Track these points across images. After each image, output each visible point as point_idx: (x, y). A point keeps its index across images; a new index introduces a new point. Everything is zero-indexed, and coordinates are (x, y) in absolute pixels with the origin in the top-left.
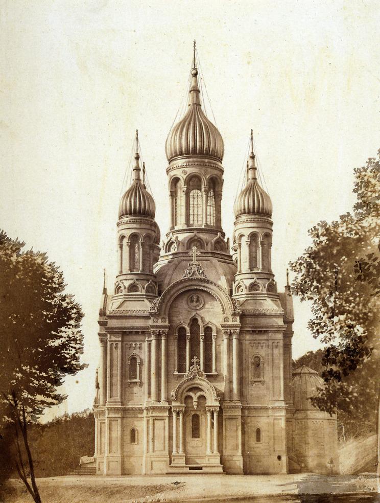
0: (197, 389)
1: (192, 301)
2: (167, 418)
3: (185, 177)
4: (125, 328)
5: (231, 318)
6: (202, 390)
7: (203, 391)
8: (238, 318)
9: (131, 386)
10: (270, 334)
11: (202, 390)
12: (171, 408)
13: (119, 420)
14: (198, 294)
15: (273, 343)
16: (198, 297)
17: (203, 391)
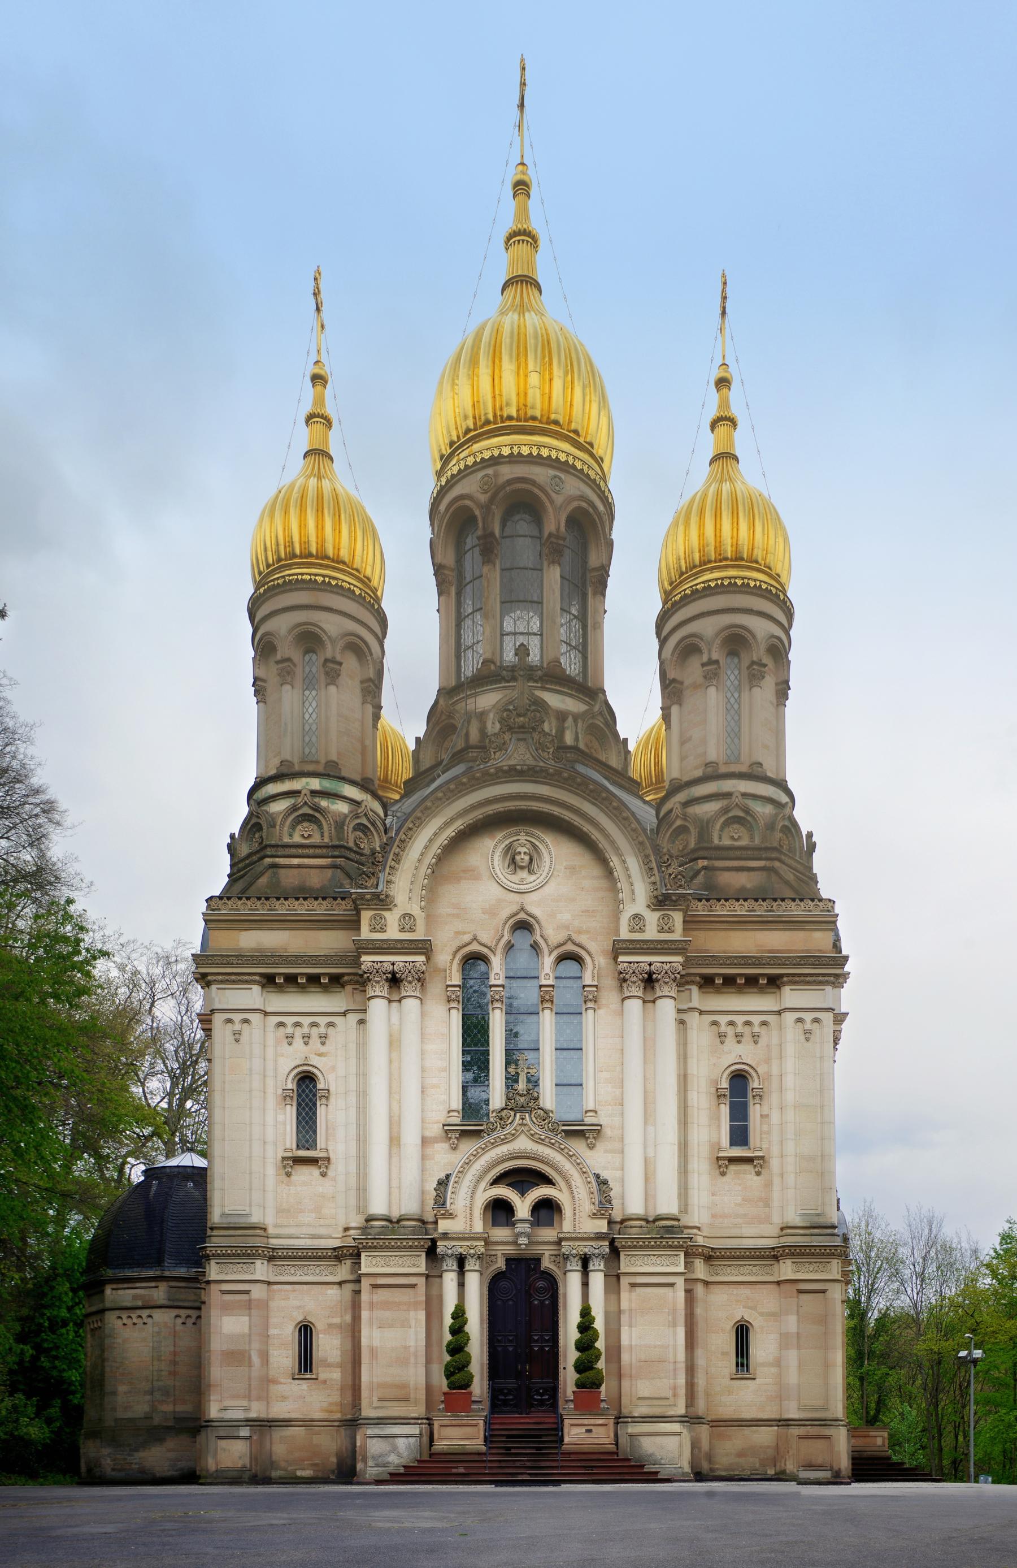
0: (522, 1177)
7: (554, 1184)
10: (786, 990)
11: (548, 1181)
15: (799, 1020)
17: (554, 1184)
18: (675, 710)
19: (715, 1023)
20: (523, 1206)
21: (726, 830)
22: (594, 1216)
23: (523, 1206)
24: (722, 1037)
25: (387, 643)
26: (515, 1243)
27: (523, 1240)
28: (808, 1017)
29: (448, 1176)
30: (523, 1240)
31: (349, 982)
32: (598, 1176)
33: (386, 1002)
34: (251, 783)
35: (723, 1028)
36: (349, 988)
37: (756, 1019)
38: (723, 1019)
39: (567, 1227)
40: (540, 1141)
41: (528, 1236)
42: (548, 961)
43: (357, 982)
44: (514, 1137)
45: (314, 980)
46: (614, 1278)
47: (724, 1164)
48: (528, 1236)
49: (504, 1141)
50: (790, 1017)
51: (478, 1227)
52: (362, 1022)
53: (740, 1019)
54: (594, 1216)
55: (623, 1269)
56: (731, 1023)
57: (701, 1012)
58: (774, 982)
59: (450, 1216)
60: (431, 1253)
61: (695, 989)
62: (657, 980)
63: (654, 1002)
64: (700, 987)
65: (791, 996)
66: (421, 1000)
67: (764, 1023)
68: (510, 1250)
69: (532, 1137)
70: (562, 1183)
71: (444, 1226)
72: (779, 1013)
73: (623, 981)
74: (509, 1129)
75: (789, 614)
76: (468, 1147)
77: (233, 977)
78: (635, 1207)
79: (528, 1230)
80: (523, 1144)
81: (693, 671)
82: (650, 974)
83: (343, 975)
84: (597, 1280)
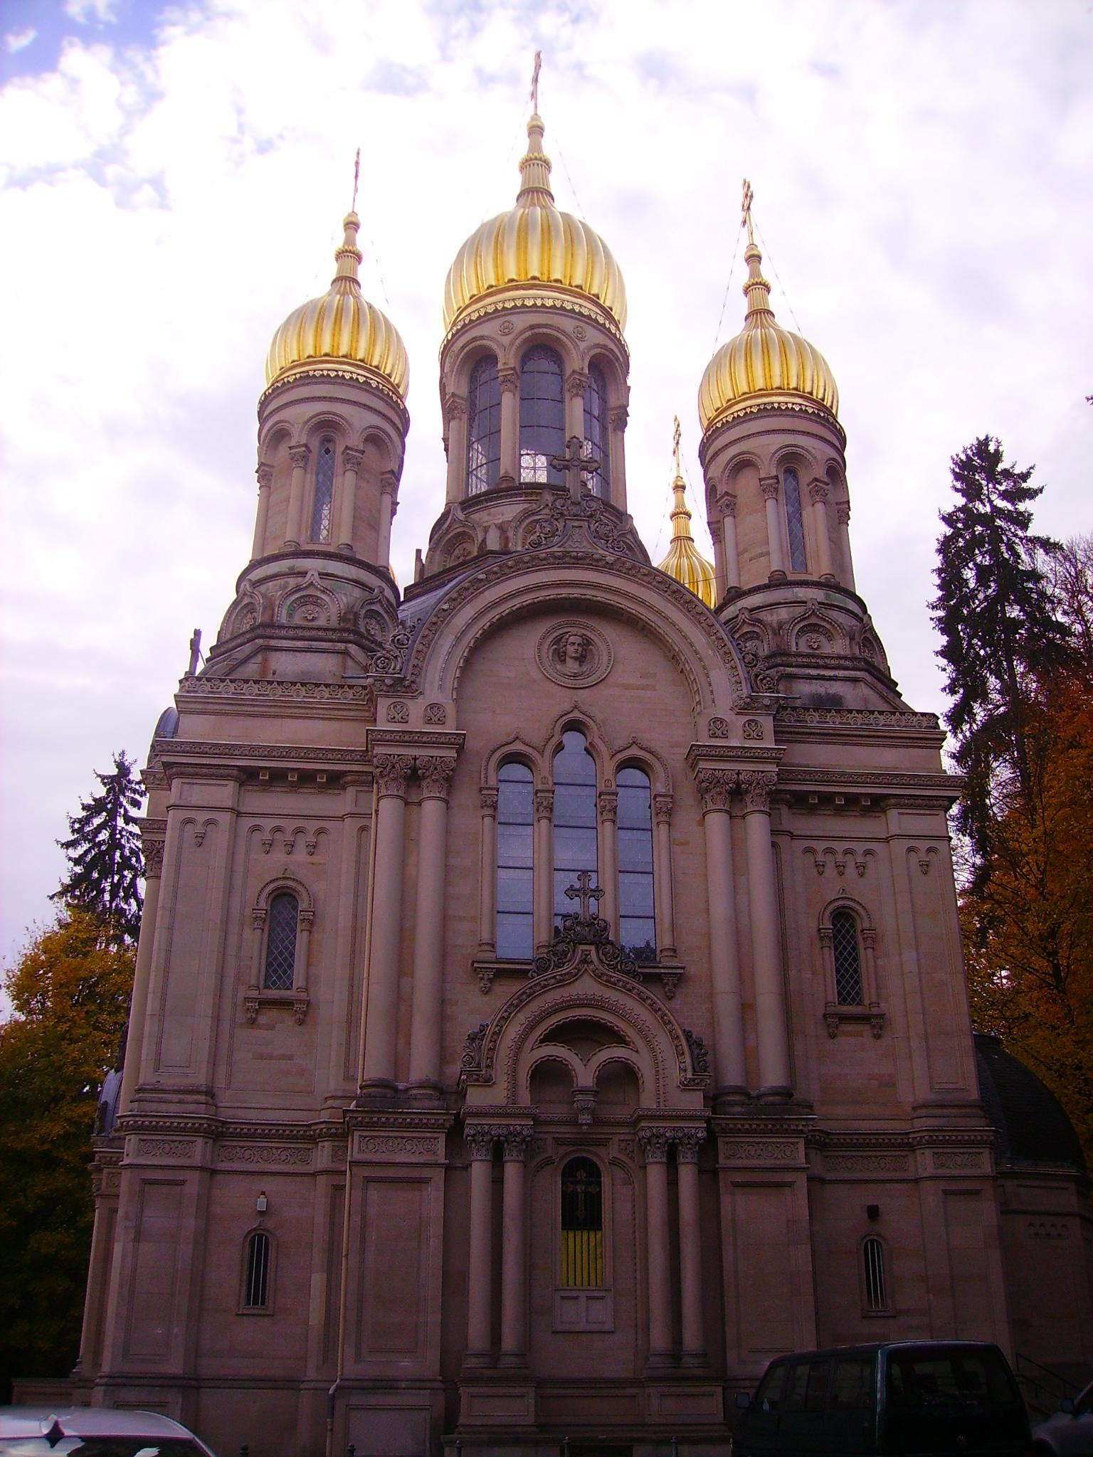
0: (585, 1032)
1: (561, 657)
2: (439, 1175)
3: (506, 340)
4: (252, 751)
5: (737, 722)
6: (618, 1038)
7: (627, 1043)
8: (767, 723)
9: (263, 1019)
10: (893, 813)
11: (618, 1038)
12: (459, 1123)
13: (194, 1183)
14: (586, 627)
15: (911, 850)
16: (587, 643)
17: (627, 1043)
18: (728, 521)
19: (809, 850)
20: (585, 1073)
21: (805, 638)
22: (686, 1086)
23: (585, 1073)
24: (820, 867)
25: (407, 440)
26: (575, 1123)
27: (585, 1118)
28: (923, 845)
29: (483, 1028)
30: (585, 1118)
31: (354, 783)
32: (688, 1035)
33: (398, 803)
34: (245, 564)
35: (820, 858)
36: (351, 791)
37: (860, 847)
38: (820, 846)
39: (648, 1101)
40: (611, 984)
41: (592, 1112)
42: (609, 766)
43: (362, 783)
44: (575, 976)
45: (307, 778)
46: (709, 1173)
47: (835, 1022)
48: (592, 1112)
49: (561, 983)
50: (899, 846)
51: (525, 1098)
52: (364, 829)
53: (840, 846)
54: (686, 1086)
55: (722, 1161)
56: (828, 851)
57: (793, 837)
58: (877, 805)
59: (488, 1082)
60: (455, 1134)
61: (784, 809)
62: (747, 791)
63: (743, 817)
64: (790, 808)
65: (897, 821)
66: (447, 802)
67: (868, 852)
68: (566, 1131)
69: (598, 976)
70: (640, 1043)
71: (476, 1097)
72: (887, 840)
73: (702, 793)
74: (567, 968)
75: (843, 441)
76: (507, 990)
77: (205, 771)
78: (732, 1076)
79: (591, 1105)
80: (586, 987)
81: (747, 485)
82: (738, 784)
83: (345, 773)
84: (687, 1175)
